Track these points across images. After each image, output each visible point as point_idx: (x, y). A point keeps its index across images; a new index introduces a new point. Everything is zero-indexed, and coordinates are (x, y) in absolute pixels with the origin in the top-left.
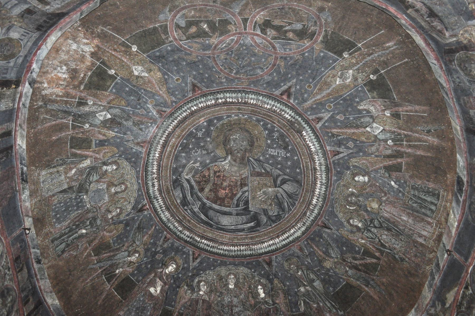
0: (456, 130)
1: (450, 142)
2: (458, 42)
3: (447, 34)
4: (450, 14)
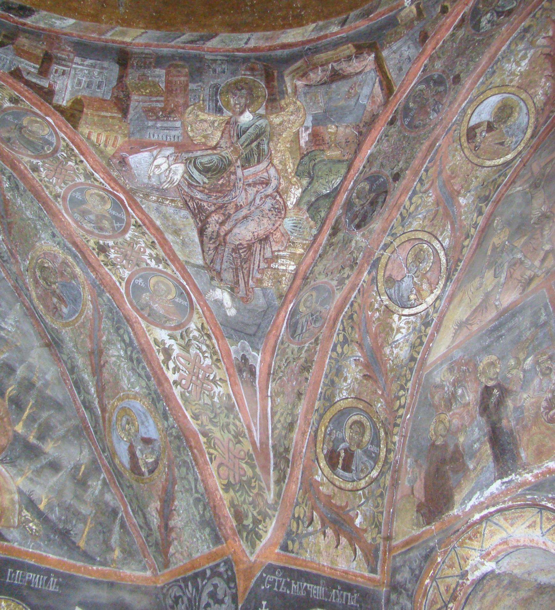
0: (124, 34)
1: (92, 12)
2: (283, 93)
3: (299, 83)
4: (330, 99)
